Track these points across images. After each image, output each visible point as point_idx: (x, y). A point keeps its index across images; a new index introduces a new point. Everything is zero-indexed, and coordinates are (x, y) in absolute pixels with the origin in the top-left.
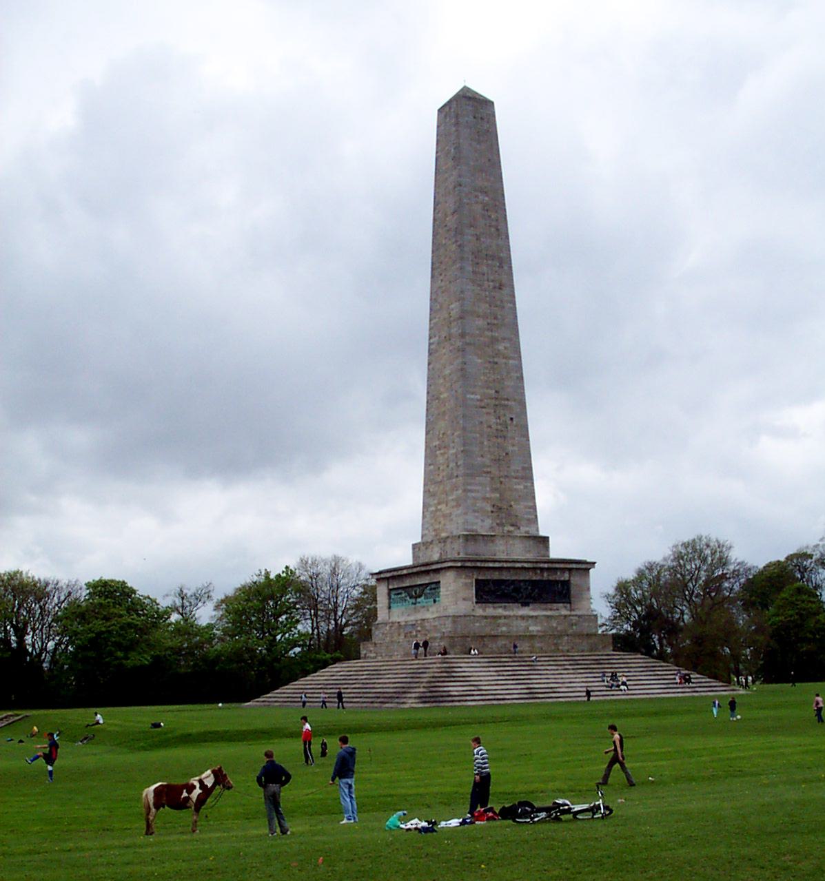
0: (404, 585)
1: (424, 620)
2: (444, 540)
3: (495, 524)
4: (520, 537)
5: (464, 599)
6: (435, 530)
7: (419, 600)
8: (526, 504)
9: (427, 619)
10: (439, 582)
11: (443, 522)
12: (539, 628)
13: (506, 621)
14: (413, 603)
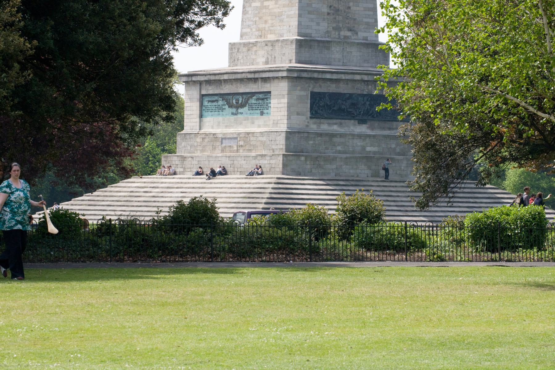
0: (222, 92)
1: (248, 134)
2: (273, 43)
3: (331, 29)
4: (358, 44)
5: (298, 114)
6: (259, 30)
7: (240, 110)
8: (365, 5)
9: (253, 133)
10: (270, 92)
11: (270, 22)
12: (375, 149)
13: (342, 140)
14: (233, 114)
